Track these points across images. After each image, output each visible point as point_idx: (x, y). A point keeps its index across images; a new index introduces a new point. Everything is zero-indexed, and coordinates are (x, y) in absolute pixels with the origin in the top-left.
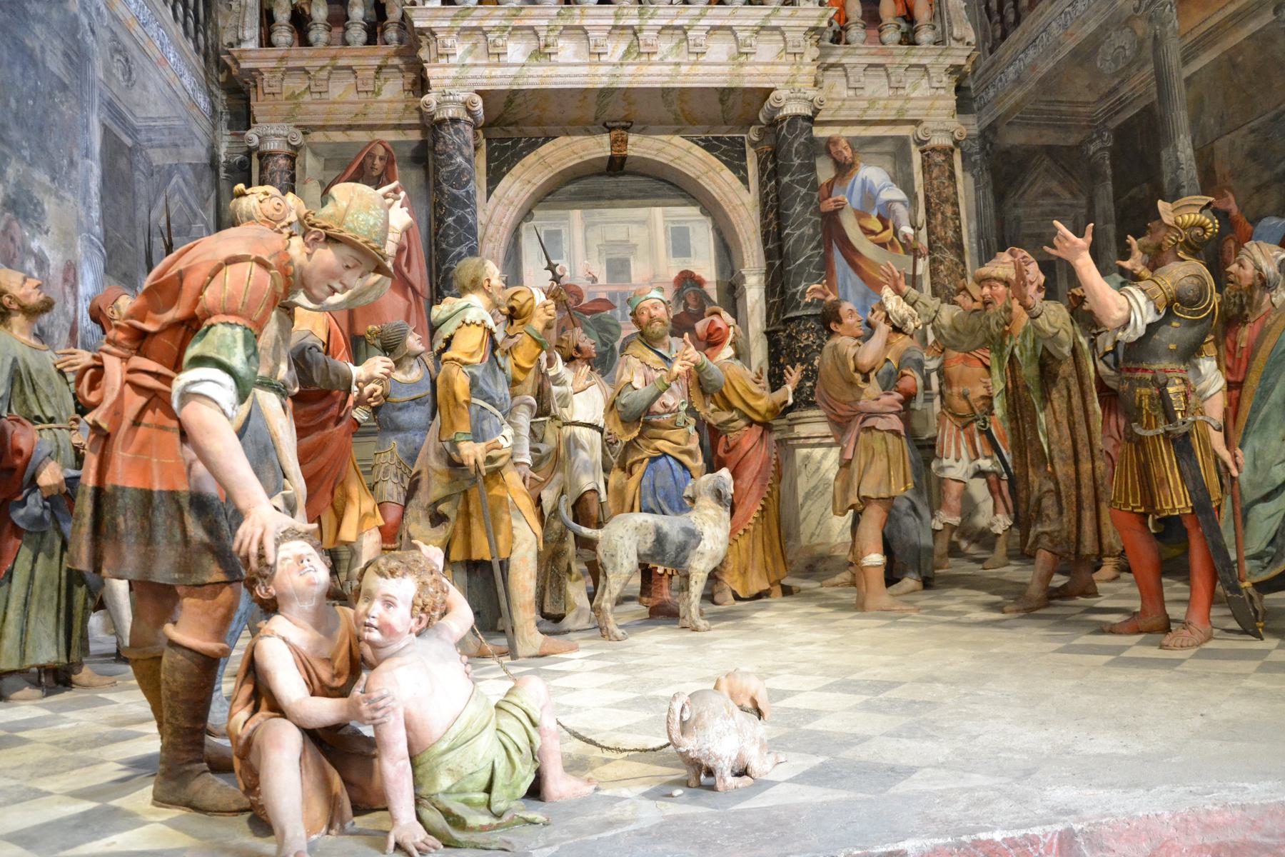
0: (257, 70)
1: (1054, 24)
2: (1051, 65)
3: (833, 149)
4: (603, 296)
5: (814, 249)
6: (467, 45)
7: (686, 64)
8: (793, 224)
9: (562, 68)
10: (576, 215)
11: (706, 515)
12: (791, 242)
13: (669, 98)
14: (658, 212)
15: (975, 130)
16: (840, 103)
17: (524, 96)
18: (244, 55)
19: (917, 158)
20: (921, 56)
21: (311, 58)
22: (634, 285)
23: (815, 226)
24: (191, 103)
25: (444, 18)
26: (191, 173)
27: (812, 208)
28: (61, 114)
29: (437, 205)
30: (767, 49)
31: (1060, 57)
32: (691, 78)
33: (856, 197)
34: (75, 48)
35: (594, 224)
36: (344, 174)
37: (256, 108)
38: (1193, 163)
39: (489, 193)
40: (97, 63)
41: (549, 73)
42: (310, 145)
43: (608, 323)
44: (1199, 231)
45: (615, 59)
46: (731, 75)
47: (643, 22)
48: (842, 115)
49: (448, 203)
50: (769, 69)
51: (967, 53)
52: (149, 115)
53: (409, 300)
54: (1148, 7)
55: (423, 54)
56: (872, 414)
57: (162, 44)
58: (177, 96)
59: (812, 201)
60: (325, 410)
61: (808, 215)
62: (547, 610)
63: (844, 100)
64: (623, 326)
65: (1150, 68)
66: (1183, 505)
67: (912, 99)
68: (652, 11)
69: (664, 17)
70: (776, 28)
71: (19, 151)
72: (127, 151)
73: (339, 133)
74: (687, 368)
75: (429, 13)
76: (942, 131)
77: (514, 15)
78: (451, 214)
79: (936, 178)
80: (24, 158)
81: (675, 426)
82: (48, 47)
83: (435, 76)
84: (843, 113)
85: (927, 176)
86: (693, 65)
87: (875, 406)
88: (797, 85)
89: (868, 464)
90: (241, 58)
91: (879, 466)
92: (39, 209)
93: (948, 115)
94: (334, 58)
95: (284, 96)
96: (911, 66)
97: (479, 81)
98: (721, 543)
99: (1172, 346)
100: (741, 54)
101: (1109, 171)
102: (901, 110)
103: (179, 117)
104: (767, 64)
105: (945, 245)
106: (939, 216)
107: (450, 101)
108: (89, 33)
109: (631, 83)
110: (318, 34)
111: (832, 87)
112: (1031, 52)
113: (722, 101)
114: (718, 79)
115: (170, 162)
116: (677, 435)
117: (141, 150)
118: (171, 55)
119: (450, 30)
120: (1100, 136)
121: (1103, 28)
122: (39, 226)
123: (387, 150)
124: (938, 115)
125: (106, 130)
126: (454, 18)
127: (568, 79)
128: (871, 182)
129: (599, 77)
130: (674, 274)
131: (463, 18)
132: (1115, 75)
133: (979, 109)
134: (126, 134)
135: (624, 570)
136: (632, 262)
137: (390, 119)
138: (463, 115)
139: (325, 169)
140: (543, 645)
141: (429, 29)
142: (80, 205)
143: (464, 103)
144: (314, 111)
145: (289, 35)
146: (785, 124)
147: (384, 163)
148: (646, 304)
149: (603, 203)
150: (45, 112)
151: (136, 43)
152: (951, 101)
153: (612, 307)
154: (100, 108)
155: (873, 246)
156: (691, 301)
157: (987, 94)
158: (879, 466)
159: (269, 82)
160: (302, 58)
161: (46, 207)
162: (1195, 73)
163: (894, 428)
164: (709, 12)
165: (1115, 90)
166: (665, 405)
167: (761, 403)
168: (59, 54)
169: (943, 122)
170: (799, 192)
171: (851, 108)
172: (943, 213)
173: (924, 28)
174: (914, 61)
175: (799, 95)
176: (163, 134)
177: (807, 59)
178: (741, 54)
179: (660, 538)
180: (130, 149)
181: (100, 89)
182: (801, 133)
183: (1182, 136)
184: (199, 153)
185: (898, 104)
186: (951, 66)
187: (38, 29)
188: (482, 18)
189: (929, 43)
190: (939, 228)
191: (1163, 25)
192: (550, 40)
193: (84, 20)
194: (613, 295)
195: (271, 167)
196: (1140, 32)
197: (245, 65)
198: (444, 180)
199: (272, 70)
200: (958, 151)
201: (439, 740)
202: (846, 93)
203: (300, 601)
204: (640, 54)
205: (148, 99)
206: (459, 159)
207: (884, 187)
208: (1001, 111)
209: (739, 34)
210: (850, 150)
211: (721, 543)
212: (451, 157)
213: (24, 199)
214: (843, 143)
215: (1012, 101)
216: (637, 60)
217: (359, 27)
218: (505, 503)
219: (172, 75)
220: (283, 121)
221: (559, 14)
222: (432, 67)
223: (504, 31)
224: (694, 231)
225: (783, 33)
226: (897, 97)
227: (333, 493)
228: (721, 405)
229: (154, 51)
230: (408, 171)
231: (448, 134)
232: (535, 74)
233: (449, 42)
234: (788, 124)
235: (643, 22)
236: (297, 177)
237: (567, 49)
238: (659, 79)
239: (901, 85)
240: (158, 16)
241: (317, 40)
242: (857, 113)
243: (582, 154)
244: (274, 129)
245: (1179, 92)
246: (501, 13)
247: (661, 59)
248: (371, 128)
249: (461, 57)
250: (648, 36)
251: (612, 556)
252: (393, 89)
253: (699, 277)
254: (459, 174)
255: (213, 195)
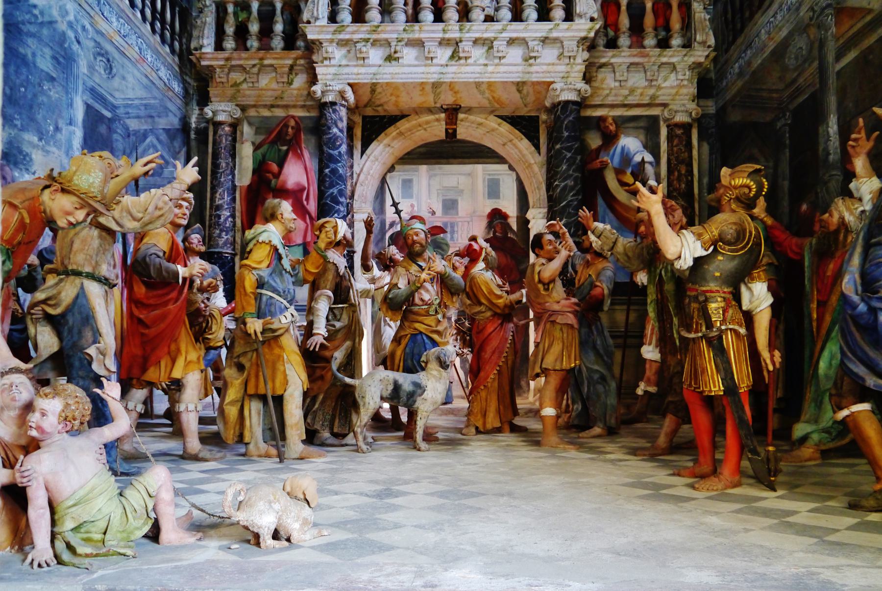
0: (212, 66)
1: (763, 31)
2: (759, 61)
3: (602, 125)
4: (439, 224)
5: (573, 196)
6: (343, 51)
7: (492, 65)
8: (560, 178)
9: (406, 68)
10: (423, 168)
11: (431, 374)
12: (558, 190)
13: (482, 89)
14: (479, 167)
15: (712, 110)
16: (608, 92)
17: (382, 87)
18: (203, 56)
19: (664, 132)
20: (671, 56)
21: (246, 59)
22: (460, 217)
23: (575, 179)
24: (166, 89)
25: (328, 33)
26: (165, 135)
27: (574, 167)
28: (49, 97)
29: (321, 162)
30: (549, 54)
31: (765, 56)
32: (494, 75)
33: (617, 159)
34: (63, 53)
35: (435, 175)
36: (268, 138)
37: (212, 91)
38: (838, 137)
39: (363, 153)
40: (81, 63)
41: (397, 71)
42: (246, 118)
43: (441, 243)
44: (746, 190)
45: (443, 62)
46: (523, 73)
47: (462, 35)
48: (610, 100)
49: (326, 160)
50: (550, 68)
51: (706, 53)
52: (127, 97)
53: (306, 222)
54: (818, 17)
55: (315, 58)
56: (555, 312)
57: (140, 49)
58: (154, 84)
59: (575, 162)
60: (168, 294)
61: (571, 172)
62: (335, 430)
63: (611, 89)
64: (451, 245)
65: (816, 64)
66: (717, 389)
67: (663, 88)
68: (468, 27)
69: (477, 31)
70: (556, 40)
71: (12, 121)
72: (107, 121)
73: (266, 110)
74: (431, 276)
75: (317, 29)
76: (682, 111)
77: (374, 31)
78: (328, 167)
79: (676, 146)
80: (16, 126)
81: (427, 314)
82: (39, 53)
83: (321, 73)
84: (610, 98)
85: (670, 144)
86: (496, 65)
87: (556, 307)
88: (570, 80)
89: (550, 346)
90: (201, 58)
91: (556, 348)
92: (28, 159)
93: (689, 100)
94: (261, 59)
95: (230, 84)
96: (663, 64)
97: (350, 76)
98: (440, 393)
99: (717, 274)
100: (531, 58)
101: (787, 142)
102: (653, 97)
103: (155, 98)
104: (549, 64)
105: (679, 194)
106: (676, 173)
107: (330, 91)
108: (75, 43)
109: (453, 78)
110: (253, 43)
111: (603, 81)
112: (749, 52)
113: (519, 91)
114: (513, 75)
115: (145, 127)
116: (430, 321)
117: (120, 120)
118: (149, 56)
119: (331, 41)
120: (784, 115)
121: (791, 34)
122: (27, 169)
123: (296, 122)
124: (682, 100)
125: (88, 108)
126: (335, 32)
127: (410, 76)
128: (629, 149)
129: (430, 74)
130: (488, 210)
131: (340, 32)
132: (796, 69)
133: (717, 95)
134: (107, 109)
135: (370, 407)
136: (459, 202)
137: (298, 101)
138: (339, 100)
139: (257, 132)
140: (302, 452)
141: (318, 40)
142: (64, 156)
143: (340, 92)
144: (248, 94)
145: (233, 42)
146: (560, 107)
147: (294, 131)
148: (411, 232)
149: (442, 161)
150: (35, 95)
151: (117, 48)
152: (693, 90)
153: (444, 232)
154: (83, 92)
155: (625, 194)
156: (498, 229)
157: (722, 84)
158: (556, 348)
159: (220, 76)
160: (240, 59)
161: (34, 156)
162: (842, 69)
163: (570, 322)
164: (509, 27)
165: (794, 81)
166: (422, 300)
167: (501, 301)
168: (48, 57)
169: (684, 105)
170: (566, 155)
171: (616, 95)
172: (679, 171)
173: (676, 35)
174: (664, 60)
175: (570, 86)
176: (140, 110)
177: (579, 60)
178: (531, 58)
179: (397, 387)
180: (109, 119)
181: (83, 80)
182: (571, 113)
183: (832, 116)
184: (174, 121)
185: (651, 91)
186: (694, 63)
187: (30, 41)
188: (353, 33)
189: (679, 46)
190: (675, 182)
191: (827, 31)
192: (398, 48)
193: (71, 34)
194: (446, 224)
195: (220, 132)
196: (812, 36)
197: (204, 63)
198: (325, 144)
199: (221, 67)
200: (696, 125)
201: (67, 499)
202: (613, 84)
203: (8, 410)
204: (460, 58)
205: (127, 87)
206: (335, 130)
207: (637, 152)
208: (728, 96)
209: (530, 43)
210: (614, 125)
211: (440, 393)
212: (329, 128)
213: (15, 152)
214: (610, 120)
215: (736, 89)
216: (458, 63)
217: (279, 38)
218: (281, 359)
219: (149, 70)
220: (228, 101)
221: (404, 30)
222: (319, 66)
223: (367, 42)
224: (503, 181)
225: (562, 42)
226: (651, 86)
227: (169, 347)
228: (475, 302)
229: (133, 53)
230: (309, 137)
231: (330, 114)
232: (388, 72)
233: (330, 49)
234: (561, 108)
235: (462, 35)
236: (238, 139)
237: (409, 55)
238: (473, 75)
239: (655, 78)
240: (137, 30)
241: (251, 46)
242: (621, 98)
243: (425, 127)
244: (222, 106)
245: (832, 82)
246: (365, 29)
247: (475, 61)
248: (286, 107)
249: (339, 60)
250: (466, 45)
251: (363, 397)
252: (300, 81)
253: (505, 213)
254: (335, 140)
255: (184, 150)
